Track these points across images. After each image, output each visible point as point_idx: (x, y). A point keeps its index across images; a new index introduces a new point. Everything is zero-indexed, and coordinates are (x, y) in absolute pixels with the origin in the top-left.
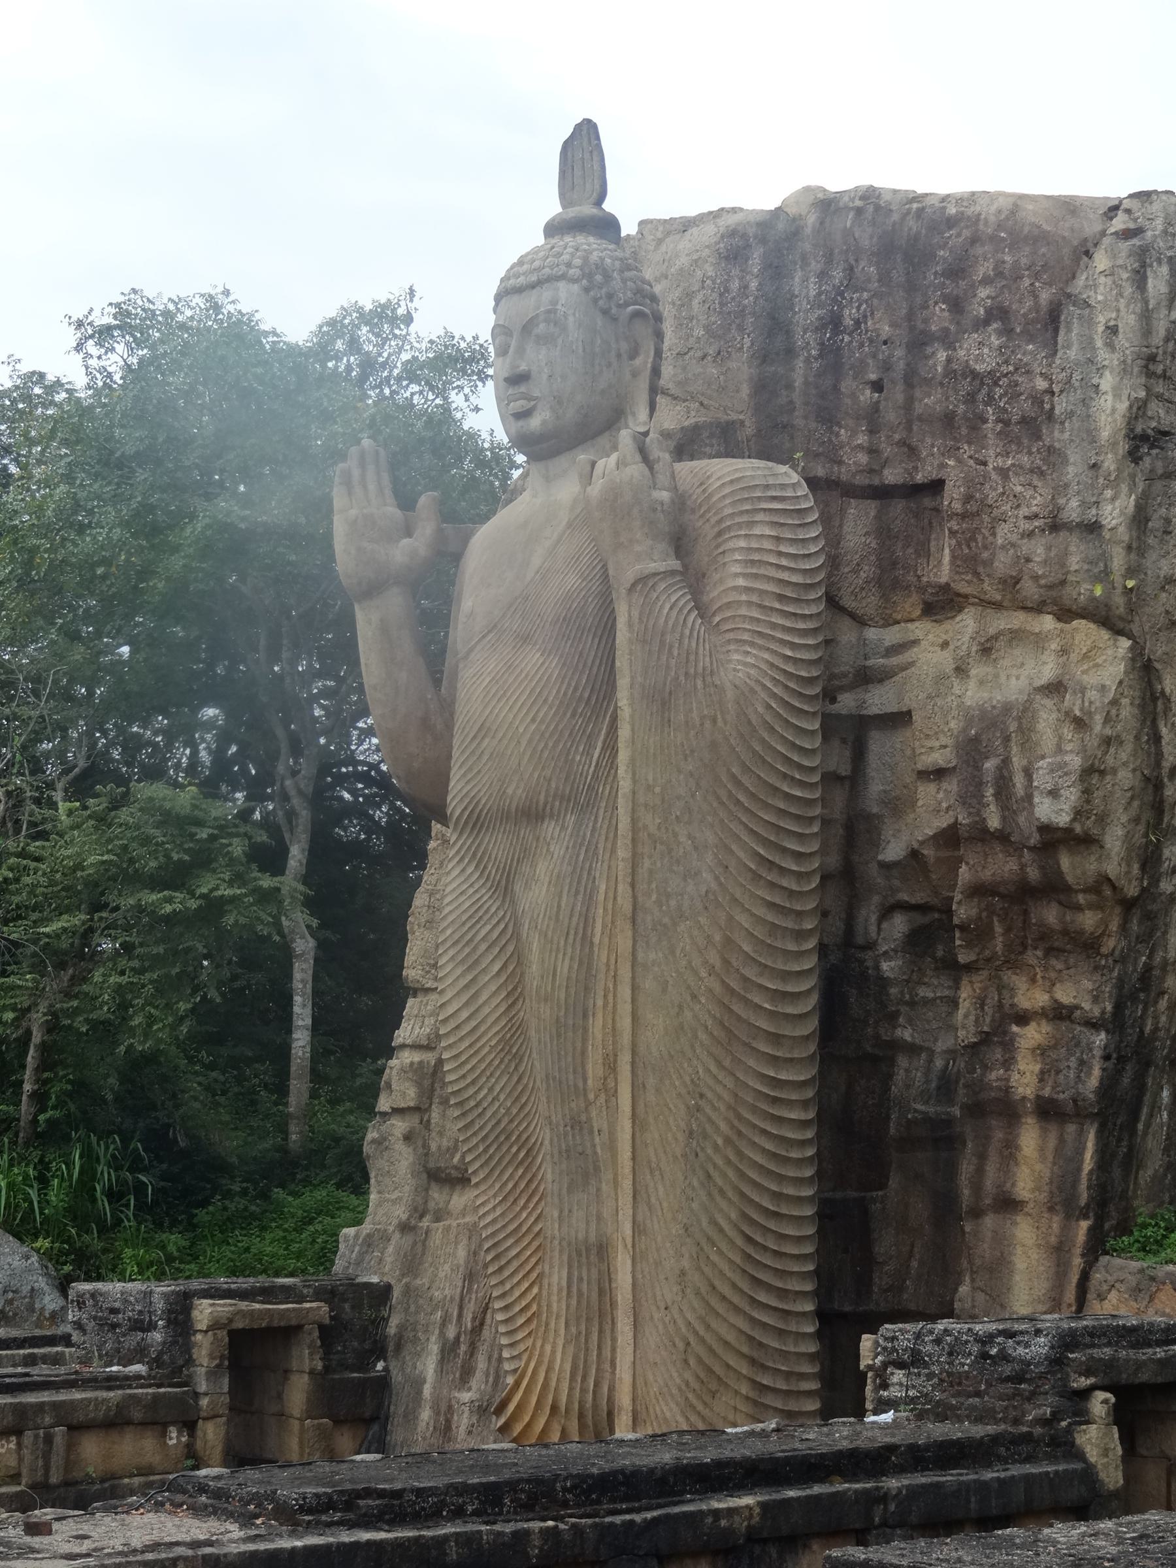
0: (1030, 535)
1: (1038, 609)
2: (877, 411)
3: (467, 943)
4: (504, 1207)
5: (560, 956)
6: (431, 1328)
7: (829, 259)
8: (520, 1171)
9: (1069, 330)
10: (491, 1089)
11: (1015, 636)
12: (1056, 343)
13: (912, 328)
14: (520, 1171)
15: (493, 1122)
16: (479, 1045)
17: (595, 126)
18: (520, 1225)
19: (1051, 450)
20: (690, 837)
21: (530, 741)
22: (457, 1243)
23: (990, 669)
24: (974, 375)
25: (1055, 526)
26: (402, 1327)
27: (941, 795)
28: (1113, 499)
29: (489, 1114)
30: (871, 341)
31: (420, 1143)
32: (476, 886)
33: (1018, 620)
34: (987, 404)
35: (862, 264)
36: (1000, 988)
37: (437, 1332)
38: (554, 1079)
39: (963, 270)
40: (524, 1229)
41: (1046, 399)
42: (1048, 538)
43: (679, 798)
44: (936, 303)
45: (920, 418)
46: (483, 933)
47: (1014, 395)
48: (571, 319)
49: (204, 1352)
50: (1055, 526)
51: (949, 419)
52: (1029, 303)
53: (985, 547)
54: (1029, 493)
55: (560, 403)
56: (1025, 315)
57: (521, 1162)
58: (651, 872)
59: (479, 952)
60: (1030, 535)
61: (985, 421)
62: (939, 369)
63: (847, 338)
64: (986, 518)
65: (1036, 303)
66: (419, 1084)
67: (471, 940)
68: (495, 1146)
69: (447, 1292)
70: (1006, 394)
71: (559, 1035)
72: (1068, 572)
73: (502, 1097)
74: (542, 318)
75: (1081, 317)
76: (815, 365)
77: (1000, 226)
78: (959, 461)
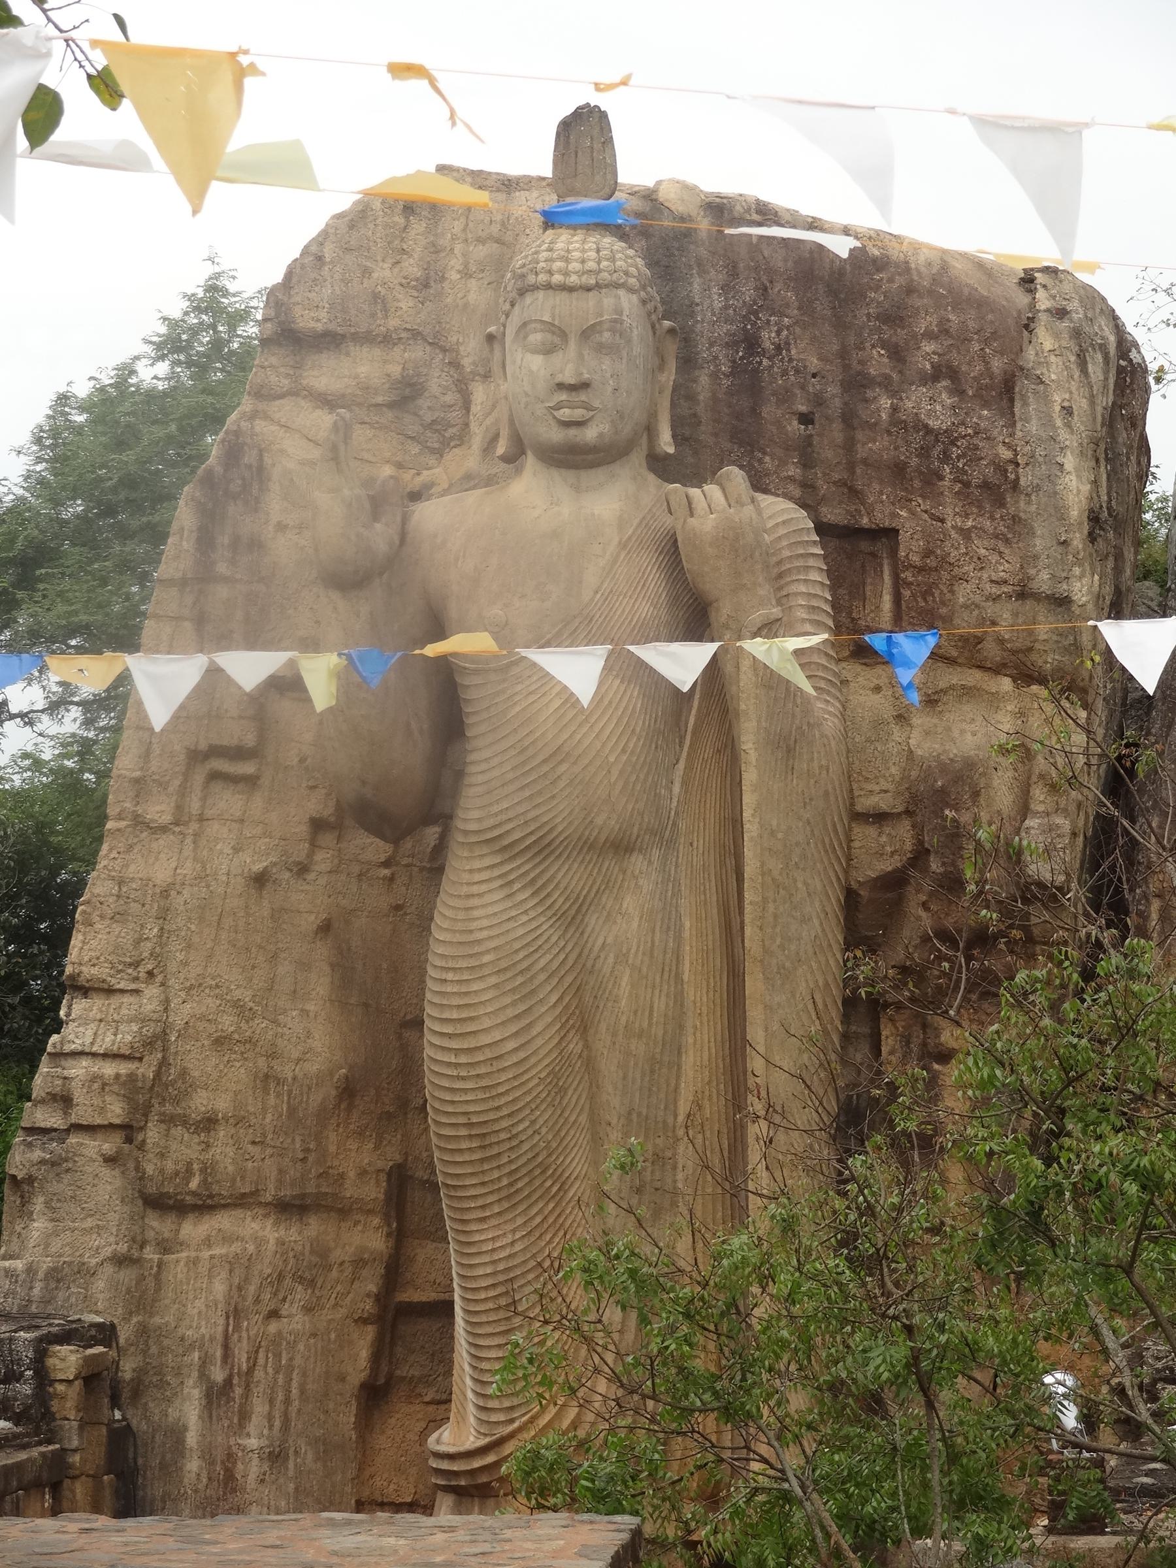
0: (996, 599)
1: (997, 670)
2: (810, 445)
3: (521, 972)
4: (526, 1242)
5: (657, 992)
6: (185, 1371)
7: (733, 272)
8: (551, 1205)
9: (1025, 404)
10: (533, 1122)
11: (968, 692)
12: (1013, 414)
13: (846, 367)
14: (551, 1205)
15: (530, 1155)
16: (526, 1077)
17: (603, 116)
19: (1016, 519)
20: (806, 884)
21: (621, 772)
22: (210, 1277)
23: (935, 721)
24: (928, 430)
25: (1023, 594)
26: (141, 1372)
27: (884, 839)
28: (1080, 578)
29: (526, 1147)
30: (797, 371)
31: (131, 1165)
32: (532, 914)
33: (973, 677)
34: (942, 462)
35: (778, 286)
36: (924, 1026)
37: (195, 1374)
38: (639, 1114)
39: (901, 319)
41: (1010, 468)
42: (1014, 604)
43: (797, 844)
44: (873, 346)
45: (865, 462)
46: (542, 963)
47: (973, 455)
48: (635, 332)
49: (69, 1404)
50: (1023, 594)
51: (899, 470)
52: (979, 368)
53: (943, 603)
54: (994, 558)
55: (622, 417)
56: (974, 378)
58: (776, 916)
59: (536, 982)
60: (996, 599)
61: (941, 478)
62: (884, 416)
63: (765, 362)
64: (945, 575)
65: (988, 369)
66: (129, 1099)
67: (527, 969)
68: (527, 1180)
69: (203, 1330)
70: (964, 455)
71: (652, 1072)
72: (1036, 641)
73: (544, 1130)
74: (606, 326)
75: (1035, 393)
76: (726, 382)
77: (935, 280)
78: (912, 513)
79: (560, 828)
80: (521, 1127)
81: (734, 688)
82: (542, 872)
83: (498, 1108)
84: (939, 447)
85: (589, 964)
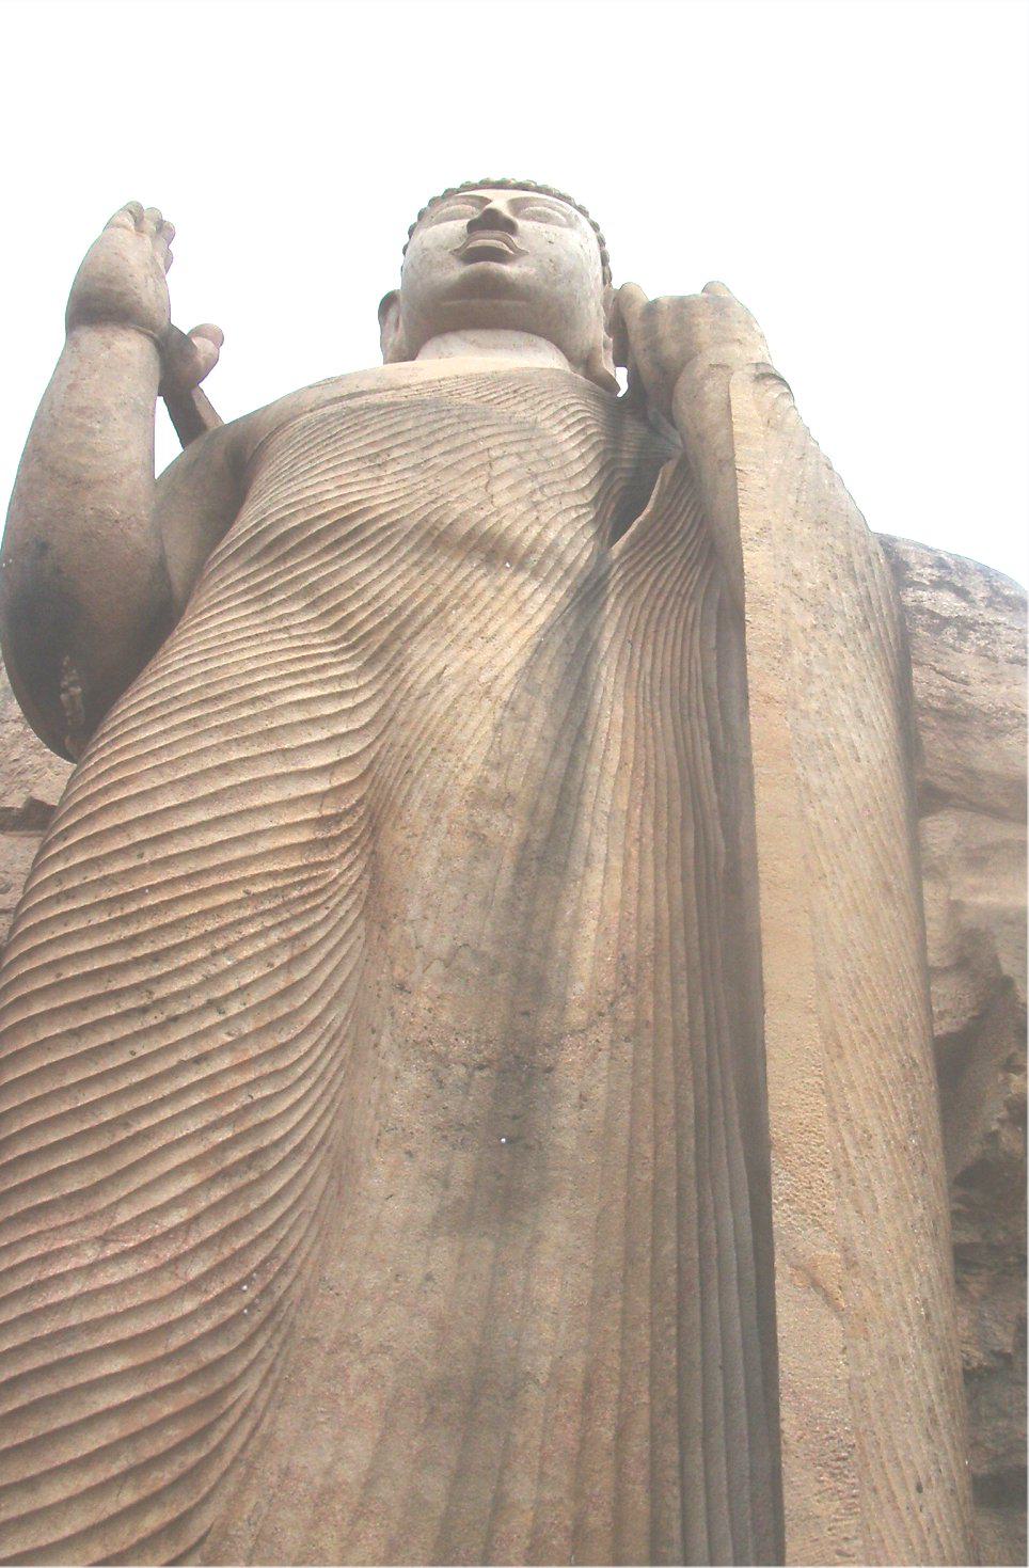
8: (218, 1193)
14: (218, 1193)
18: (168, 1328)
24: (933, 615)
40: (177, 1340)
57: (226, 1174)
79: (382, 511)
80: (179, 984)
81: (720, 438)
82: (334, 575)
83: (134, 941)
84: (951, 630)
85: (402, 715)
